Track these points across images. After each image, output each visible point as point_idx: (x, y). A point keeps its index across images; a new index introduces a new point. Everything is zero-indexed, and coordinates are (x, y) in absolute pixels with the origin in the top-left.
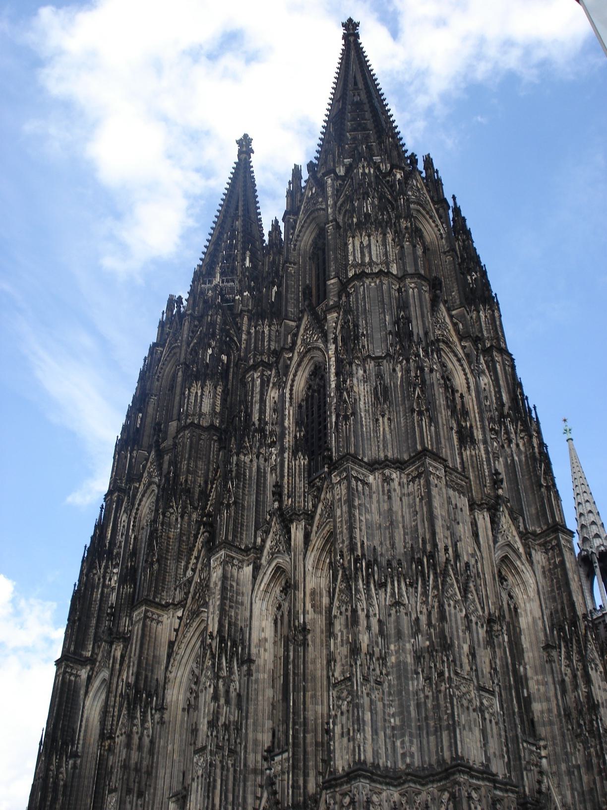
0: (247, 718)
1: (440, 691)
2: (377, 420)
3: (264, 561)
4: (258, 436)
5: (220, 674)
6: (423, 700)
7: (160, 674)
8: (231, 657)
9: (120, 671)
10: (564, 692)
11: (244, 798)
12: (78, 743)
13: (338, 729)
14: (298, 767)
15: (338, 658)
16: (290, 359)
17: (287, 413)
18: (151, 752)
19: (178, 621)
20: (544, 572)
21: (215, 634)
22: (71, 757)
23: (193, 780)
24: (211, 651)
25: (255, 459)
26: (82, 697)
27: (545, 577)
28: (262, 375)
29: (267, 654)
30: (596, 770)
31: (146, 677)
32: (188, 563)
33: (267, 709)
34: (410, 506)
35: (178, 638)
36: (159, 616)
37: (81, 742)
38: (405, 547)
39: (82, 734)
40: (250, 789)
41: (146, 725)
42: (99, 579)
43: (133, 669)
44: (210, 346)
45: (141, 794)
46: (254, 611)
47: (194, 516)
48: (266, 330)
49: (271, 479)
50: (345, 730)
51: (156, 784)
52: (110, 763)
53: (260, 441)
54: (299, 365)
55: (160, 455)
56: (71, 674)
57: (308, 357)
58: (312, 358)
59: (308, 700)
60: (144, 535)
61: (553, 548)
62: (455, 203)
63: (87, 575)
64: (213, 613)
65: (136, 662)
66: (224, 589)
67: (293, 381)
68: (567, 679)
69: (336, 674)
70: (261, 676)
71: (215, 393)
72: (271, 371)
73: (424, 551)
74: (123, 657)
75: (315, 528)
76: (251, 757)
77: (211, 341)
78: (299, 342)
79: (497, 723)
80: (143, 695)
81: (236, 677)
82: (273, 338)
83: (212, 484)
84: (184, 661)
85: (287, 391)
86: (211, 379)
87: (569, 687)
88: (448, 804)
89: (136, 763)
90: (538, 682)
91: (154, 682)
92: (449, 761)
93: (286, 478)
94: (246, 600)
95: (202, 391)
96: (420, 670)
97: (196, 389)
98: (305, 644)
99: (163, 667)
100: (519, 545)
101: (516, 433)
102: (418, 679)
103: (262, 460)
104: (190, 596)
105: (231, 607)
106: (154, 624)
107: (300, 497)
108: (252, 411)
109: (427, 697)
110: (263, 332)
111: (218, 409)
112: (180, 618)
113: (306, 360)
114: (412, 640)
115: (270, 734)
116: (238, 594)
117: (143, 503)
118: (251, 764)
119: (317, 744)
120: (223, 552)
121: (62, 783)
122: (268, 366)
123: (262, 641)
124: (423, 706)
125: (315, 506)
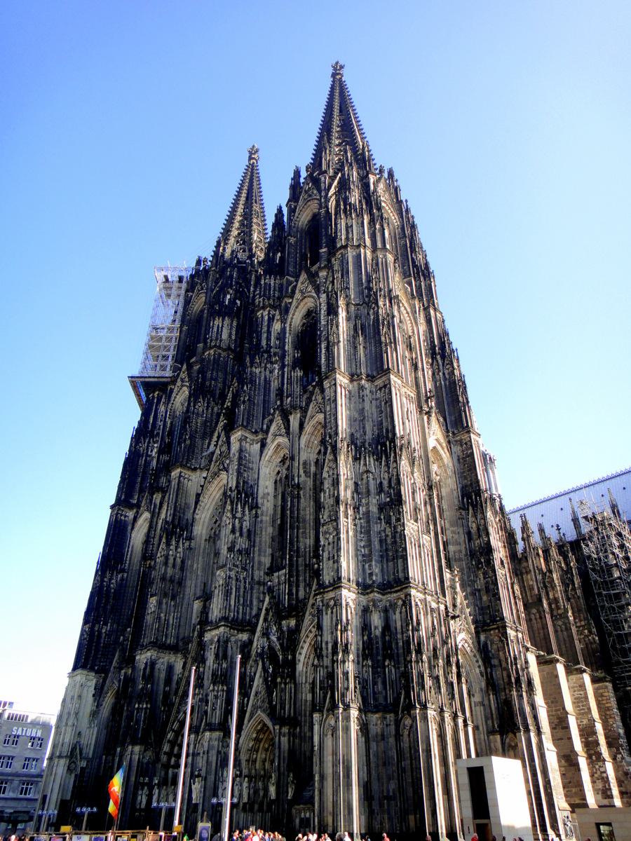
0: (254, 546)
1: (397, 532)
2: (356, 347)
3: (269, 440)
4: (266, 355)
6: (384, 538)
7: (189, 515)
8: (245, 505)
9: (159, 513)
10: (470, 539)
11: (251, 601)
12: (126, 563)
13: (326, 555)
14: (293, 581)
15: (326, 507)
16: (291, 303)
17: (287, 340)
18: (182, 569)
19: (203, 480)
20: (459, 460)
21: (233, 488)
22: (119, 573)
23: (215, 588)
24: (231, 500)
26: (129, 531)
27: (459, 463)
28: (269, 313)
29: (269, 504)
30: (491, 594)
31: (180, 517)
32: (210, 441)
34: (377, 407)
35: (203, 492)
37: (128, 562)
38: (373, 435)
39: (129, 556)
40: (255, 596)
41: (179, 550)
42: (143, 451)
43: (171, 512)
44: (228, 293)
45: (174, 598)
46: (260, 474)
47: (216, 409)
48: (272, 283)
49: (275, 385)
50: (331, 555)
51: (184, 591)
52: (152, 576)
54: (297, 307)
55: (190, 367)
56: (121, 515)
59: (300, 535)
60: (178, 424)
61: (466, 444)
63: (135, 447)
64: (232, 474)
65: (173, 507)
66: (240, 458)
67: (292, 319)
68: (472, 530)
69: (325, 517)
72: (275, 311)
73: (387, 438)
74: (161, 504)
75: (307, 420)
76: (256, 573)
77: (229, 290)
78: (297, 291)
80: (179, 527)
81: (247, 518)
82: (277, 289)
83: (229, 388)
84: (207, 507)
85: (287, 325)
87: (475, 537)
89: (171, 577)
90: (453, 532)
91: (185, 521)
92: (403, 580)
93: (285, 385)
94: (255, 466)
95: (223, 324)
96: (382, 517)
97: (218, 322)
98: (299, 497)
99: (192, 511)
101: (443, 365)
102: (381, 523)
103: (268, 373)
104: (213, 463)
105: (245, 471)
108: (261, 338)
109: (387, 536)
110: (270, 284)
111: (233, 337)
112: (205, 478)
113: (302, 304)
114: (378, 497)
115: (270, 558)
117: (176, 400)
118: (256, 578)
119: (306, 565)
120: (239, 433)
121: (113, 591)
125: (308, 405)
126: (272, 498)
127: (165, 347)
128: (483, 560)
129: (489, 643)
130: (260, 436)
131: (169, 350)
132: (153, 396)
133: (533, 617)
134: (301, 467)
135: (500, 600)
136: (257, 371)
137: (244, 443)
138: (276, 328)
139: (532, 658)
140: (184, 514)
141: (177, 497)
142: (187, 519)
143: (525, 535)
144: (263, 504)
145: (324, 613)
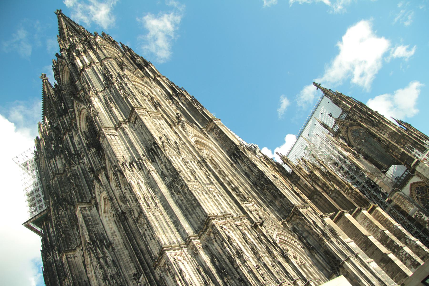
0: (121, 268)
1: (186, 193)
3: (98, 201)
5: (99, 257)
6: (181, 203)
7: (85, 278)
10: (248, 177)
15: (134, 209)
25: (79, 166)
28: (69, 135)
29: (118, 237)
30: (279, 198)
31: (79, 282)
33: (128, 259)
36: (74, 255)
42: (52, 260)
44: (52, 144)
46: (104, 223)
48: (65, 120)
53: (78, 158)
54: (80, 120)
57: (82, 114)
58: (83, 115)
61: (214, 128)
62: (121, 44)
67: (80, 128)
68: (247, 171)
70: (119, 247)
71: (61, 159)
72: (72, 131)
79: (222, 195)
81: (108, 254)
86: (57, 155)
87: (250, 174)
88: (215, 239)
91: (84, 282)
94: (99, 221)
96: (173, 191)
99: (85, 274)
100: (200, 134)
101: (179, 99)
103: (82, 165)
106: (73, 259)
107: (98, 164)
108: (70, 150)
109: (182, 200)
110: (64, 121)
113: (81, 117)
115: (135, 269)
116: (94, 221)
120: (79, 208)
122: (70, 130)
123: (113, 233)
124: (182, 205)
126: (118, 232)
127: (37, 196)
128: (262, 183)
129: (295, 226)
130: (93, 202)
131: (40, 196)
132: (44, 226)
133: (317, 200)
134: (119, 201)
135: (285, 197)
136: (76, 168)
137: (84, 212)
138: (76, 140)
139: (327, 220)
140: (81, 279)
141: (71, 271)
142: (85, 281)
143: (285, 161)
144: (114, 240)
145: (165, 276)
